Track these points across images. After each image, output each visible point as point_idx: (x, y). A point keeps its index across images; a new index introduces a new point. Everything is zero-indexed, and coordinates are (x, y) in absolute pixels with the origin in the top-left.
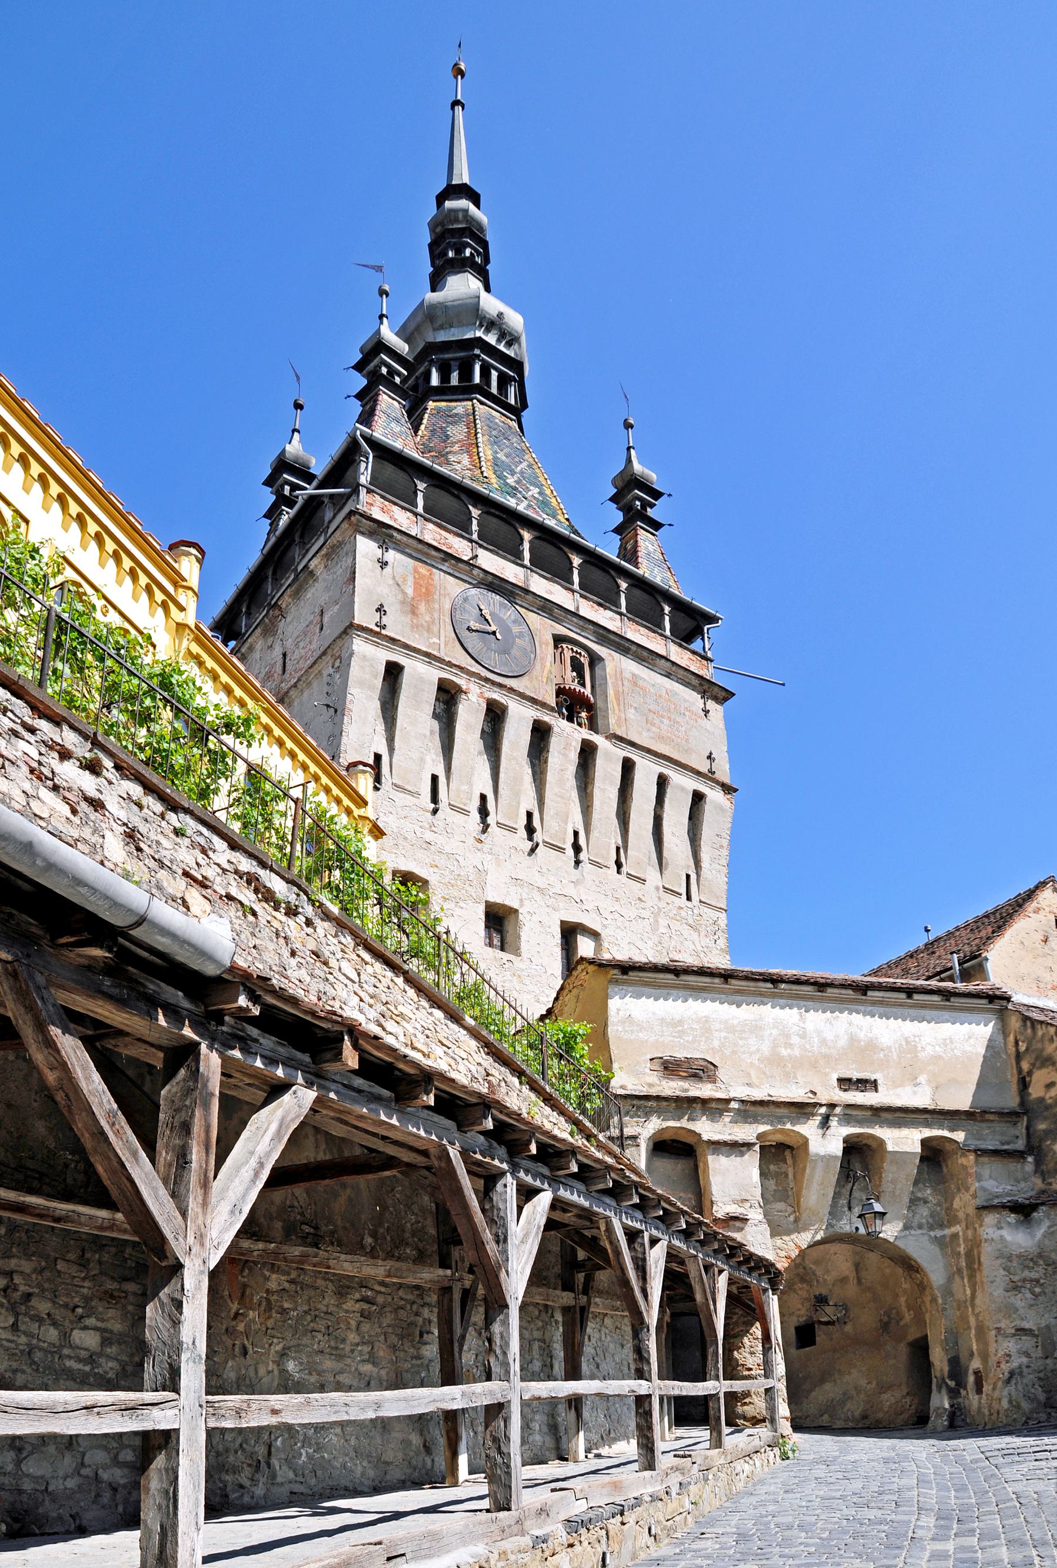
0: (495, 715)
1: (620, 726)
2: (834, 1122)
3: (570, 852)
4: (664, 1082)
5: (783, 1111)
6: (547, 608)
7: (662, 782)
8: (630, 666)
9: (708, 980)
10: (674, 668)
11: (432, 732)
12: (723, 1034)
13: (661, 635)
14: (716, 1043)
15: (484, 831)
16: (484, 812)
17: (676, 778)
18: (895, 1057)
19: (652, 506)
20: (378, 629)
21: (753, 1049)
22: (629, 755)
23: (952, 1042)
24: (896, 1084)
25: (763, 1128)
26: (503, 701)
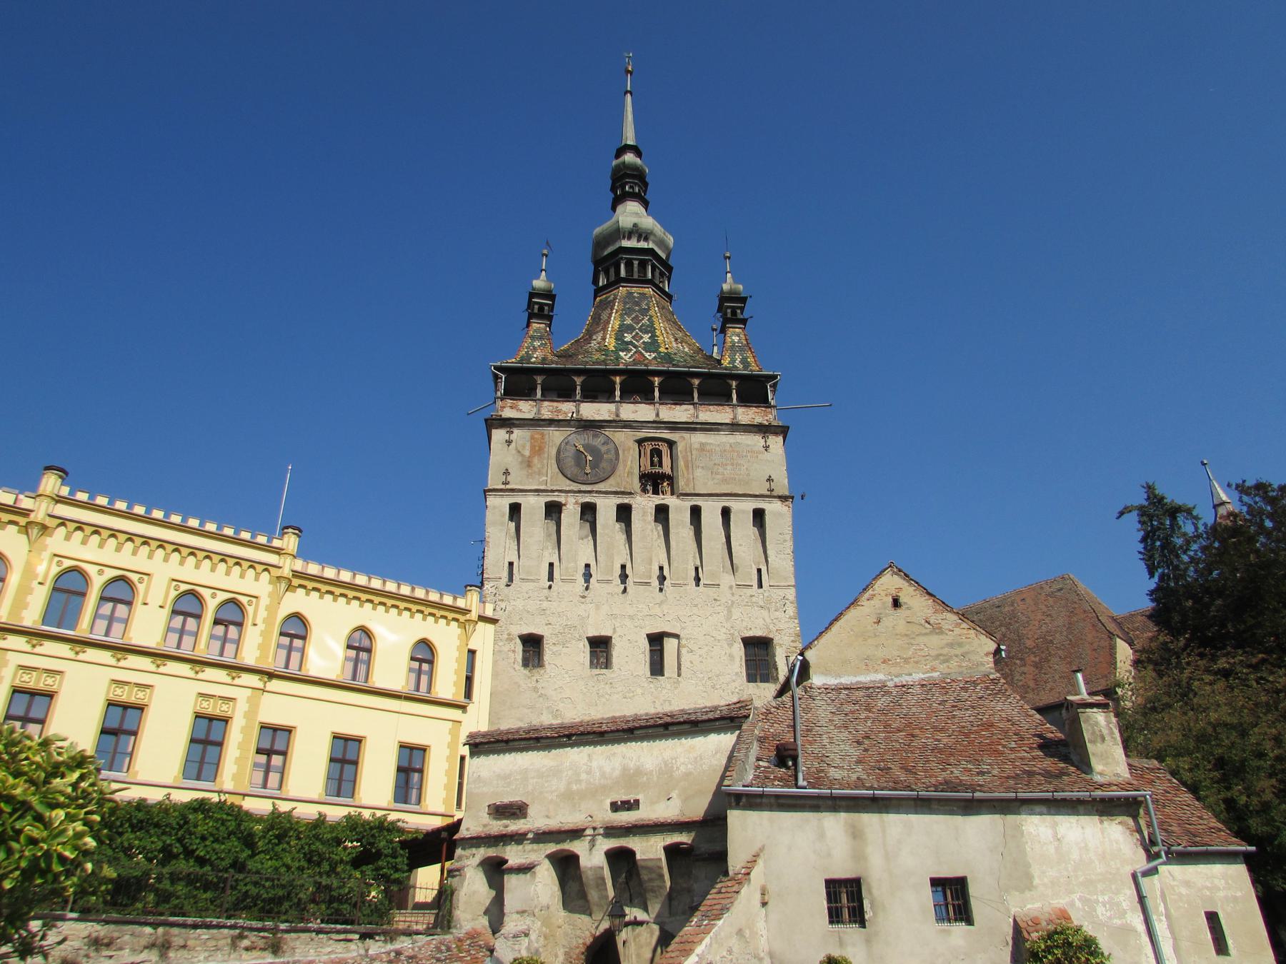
0: (588, 511)
1: (687, 485)
2: (600, 839)
3: (656, 583)
4: (495, 822)
5: (563, 836)
6: (628, 425)
7: (726, 513)
8: (698, 438)
9: (525, 742)
10: (735, 427)
11: (549, 535)
12: (535, 780)
13: (728, 405)
14: (530, 788)
15: (587, 588)
16: (588, 576)
17: (734, 505)
18: (655, 779)
19: (742, 309)
20: (503, 487)
21: (554, 788)
22: (695, 503)
23: (701, 759)
24: (653, 803)
25: (548, 852)
26: (592, 501)
